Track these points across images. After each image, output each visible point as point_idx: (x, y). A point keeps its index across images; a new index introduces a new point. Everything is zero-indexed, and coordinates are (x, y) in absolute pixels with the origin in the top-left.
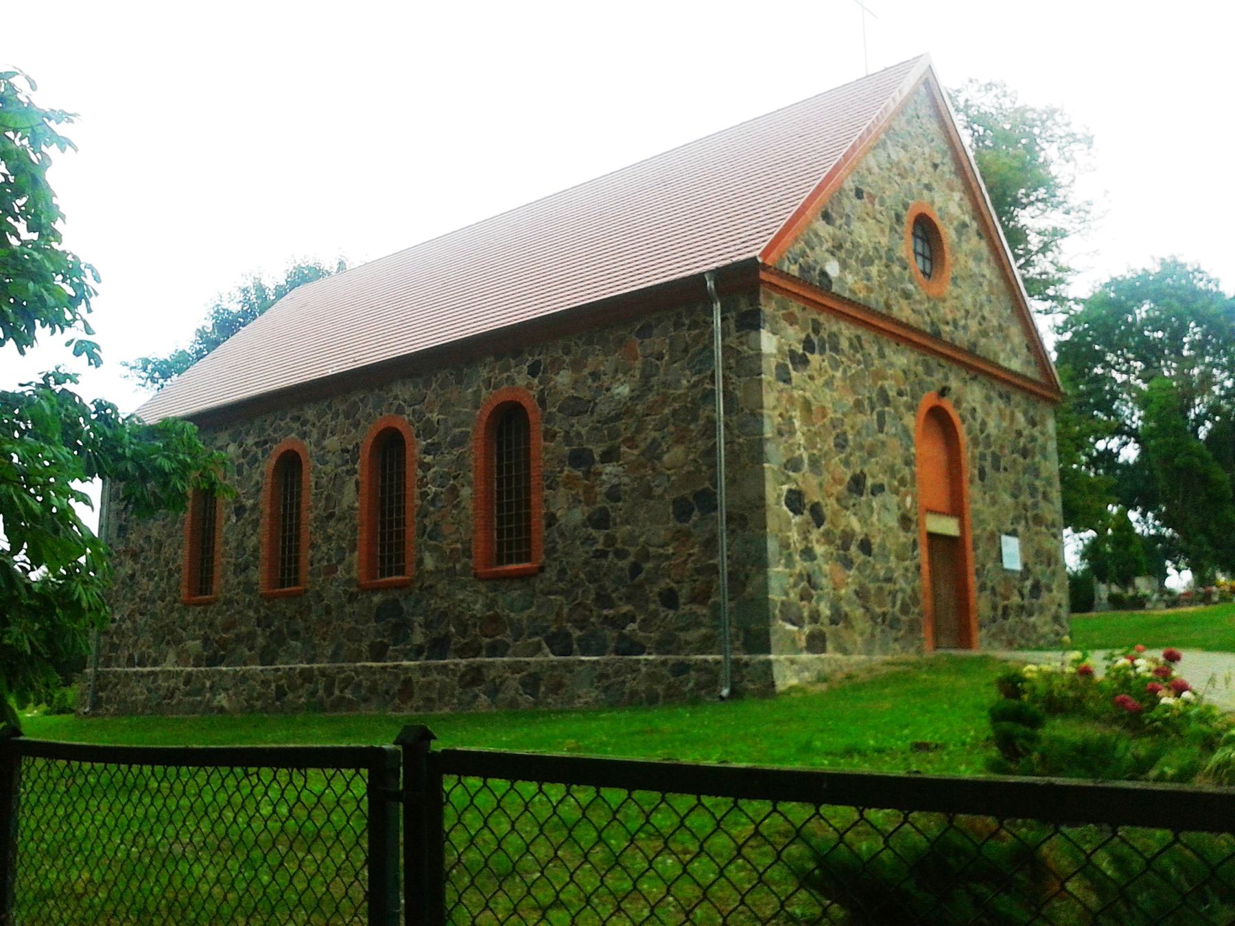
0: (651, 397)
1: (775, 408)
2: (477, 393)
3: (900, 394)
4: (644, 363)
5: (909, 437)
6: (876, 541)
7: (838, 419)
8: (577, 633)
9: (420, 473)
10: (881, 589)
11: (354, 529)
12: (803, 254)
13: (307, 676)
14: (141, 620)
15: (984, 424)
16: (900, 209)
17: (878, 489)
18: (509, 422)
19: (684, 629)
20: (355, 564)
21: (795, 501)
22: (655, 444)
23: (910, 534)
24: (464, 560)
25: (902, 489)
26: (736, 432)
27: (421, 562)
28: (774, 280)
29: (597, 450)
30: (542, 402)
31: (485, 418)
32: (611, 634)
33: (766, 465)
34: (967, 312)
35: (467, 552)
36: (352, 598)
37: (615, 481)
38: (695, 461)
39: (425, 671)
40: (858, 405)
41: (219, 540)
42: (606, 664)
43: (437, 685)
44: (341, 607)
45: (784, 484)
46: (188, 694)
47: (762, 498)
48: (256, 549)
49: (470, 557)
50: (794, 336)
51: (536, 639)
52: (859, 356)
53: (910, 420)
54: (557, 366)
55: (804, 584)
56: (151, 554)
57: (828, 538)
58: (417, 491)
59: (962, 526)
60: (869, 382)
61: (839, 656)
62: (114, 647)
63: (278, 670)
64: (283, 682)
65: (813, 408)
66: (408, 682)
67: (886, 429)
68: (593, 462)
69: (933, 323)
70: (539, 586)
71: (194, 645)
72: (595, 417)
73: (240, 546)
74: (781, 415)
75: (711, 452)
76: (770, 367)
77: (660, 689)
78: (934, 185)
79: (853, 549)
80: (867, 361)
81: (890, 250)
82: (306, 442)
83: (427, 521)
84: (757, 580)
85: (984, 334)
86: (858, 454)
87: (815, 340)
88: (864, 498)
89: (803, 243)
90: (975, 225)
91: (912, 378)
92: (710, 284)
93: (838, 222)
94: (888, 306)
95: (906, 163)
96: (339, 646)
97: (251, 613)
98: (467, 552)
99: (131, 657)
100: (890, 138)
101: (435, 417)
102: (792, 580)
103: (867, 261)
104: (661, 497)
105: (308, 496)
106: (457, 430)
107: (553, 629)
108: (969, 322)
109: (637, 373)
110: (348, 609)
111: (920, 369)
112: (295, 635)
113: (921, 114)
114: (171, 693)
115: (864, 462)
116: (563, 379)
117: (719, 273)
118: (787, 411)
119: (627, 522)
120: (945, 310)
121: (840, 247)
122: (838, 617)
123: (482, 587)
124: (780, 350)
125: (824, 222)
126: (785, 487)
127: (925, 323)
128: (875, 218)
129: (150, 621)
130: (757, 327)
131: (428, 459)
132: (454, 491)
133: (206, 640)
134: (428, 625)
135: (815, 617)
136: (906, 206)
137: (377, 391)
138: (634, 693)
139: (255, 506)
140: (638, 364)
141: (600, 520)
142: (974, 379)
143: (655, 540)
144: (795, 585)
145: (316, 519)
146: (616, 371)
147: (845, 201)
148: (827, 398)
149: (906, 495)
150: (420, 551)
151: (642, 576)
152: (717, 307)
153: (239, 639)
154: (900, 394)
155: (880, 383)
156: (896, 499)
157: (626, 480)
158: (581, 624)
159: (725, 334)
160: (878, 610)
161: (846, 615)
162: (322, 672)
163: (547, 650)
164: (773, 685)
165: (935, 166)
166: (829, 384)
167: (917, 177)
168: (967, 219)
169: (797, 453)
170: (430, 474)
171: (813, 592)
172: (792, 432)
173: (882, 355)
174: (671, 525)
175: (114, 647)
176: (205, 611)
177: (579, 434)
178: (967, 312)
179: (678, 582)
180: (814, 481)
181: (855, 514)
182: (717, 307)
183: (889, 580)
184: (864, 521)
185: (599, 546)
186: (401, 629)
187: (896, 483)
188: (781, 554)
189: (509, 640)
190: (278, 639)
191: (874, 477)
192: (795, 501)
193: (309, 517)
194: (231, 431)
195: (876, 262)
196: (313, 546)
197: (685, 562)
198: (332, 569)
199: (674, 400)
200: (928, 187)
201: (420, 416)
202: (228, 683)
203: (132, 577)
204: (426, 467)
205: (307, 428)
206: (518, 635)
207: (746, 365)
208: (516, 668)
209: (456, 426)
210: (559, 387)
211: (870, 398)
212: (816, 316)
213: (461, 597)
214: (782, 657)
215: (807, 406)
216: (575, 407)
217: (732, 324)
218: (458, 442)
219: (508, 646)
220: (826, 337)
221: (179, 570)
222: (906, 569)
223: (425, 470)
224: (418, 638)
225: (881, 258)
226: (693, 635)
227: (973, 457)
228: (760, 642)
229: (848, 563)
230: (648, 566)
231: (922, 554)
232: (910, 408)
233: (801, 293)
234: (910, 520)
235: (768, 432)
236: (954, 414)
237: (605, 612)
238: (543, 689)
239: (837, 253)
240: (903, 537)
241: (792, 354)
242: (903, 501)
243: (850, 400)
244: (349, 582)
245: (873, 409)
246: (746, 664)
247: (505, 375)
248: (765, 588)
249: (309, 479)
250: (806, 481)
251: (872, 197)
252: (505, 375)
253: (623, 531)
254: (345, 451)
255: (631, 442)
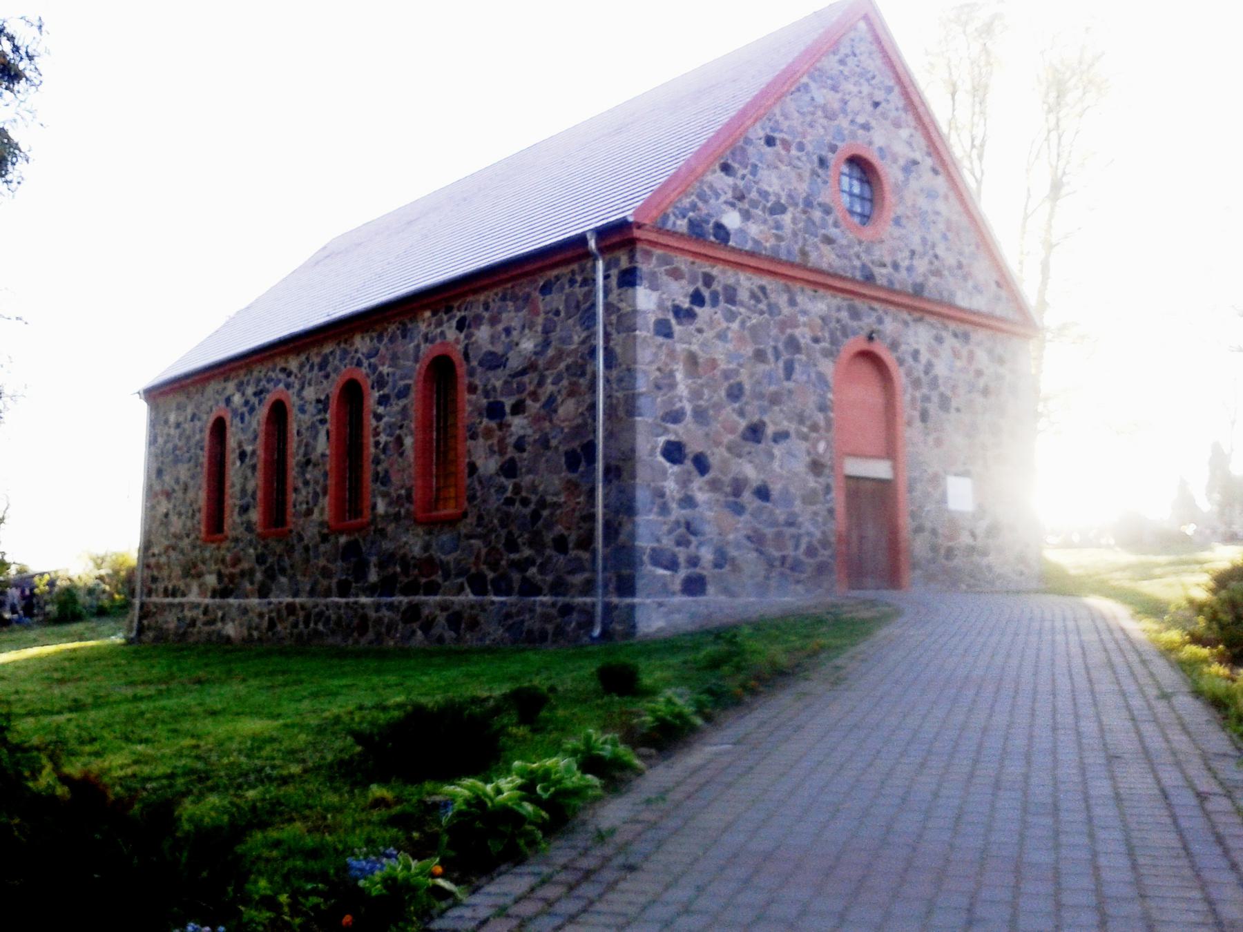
0: (551, 352)
1: (652, 362)
2: (418, 346)
3: (816, 340)
4: (546, 319)
5: (826, 383)
6: (776, 489)
7: (732, 371)
8: (491, 575)
9: (374, 423)
10: (779, 535)
11: (326, 474)
12: (694, 207)
13: (291, 608)
14: (173, 554)
15: (929, 367)
16: (825, 153)
17: (781, 436)
18: (442, 372)
19: (572, 572)
20: (325, 509)
21: (674, 452)
22: (551, 399)
23: (821, 480)
24: (407, 505)
25: (814, 435)
26: (615, 386)
27: (374, 507)
28: (653, 236)
29: (508, 403)
30: (466, 355)
31: (423, 372)
32: (516, 576)
33: (638, 419)
34: (913, 253)
35: (409, 497)
36: (325, 538)
37: (521, 432)
38: (582, 414)
39: (378, 607)
40: (760, 356)
41: (228, 484)
42: (512, 605)
43: (386, 620)
44: (316, 546)
45: (658, 435)
46: (205, 624)
47: (633, 450)
48: (254, 493)
49: (411, 502)
50: (679, 293)
51: (460, 580)
52: (762, 306)
53: (827, 367)
54: (478, 320)
55: (682, 530)
56: (179, 494)
57: (714, 485)
58: (372, 440)
59: (895, 468)
60: (774, 332)
61: (722, 598)
62: (154, 579)
63: (270, 603)
64: (274, 614)
65: (701, 360)
66: (364, 618)
67: (794, 376)
68: (503, 414)
69: (864, 266)
70: (464, 531)
71: (211, 580)
72: (507, 372)
73: (243, 491)
74: (659, 369)
75: (593, 407)
76: (647, 324)
77: (550, 627)
78: (873, 123)
79: (747, 496)
80: (773, 309)
81: (809, 195)
82: (290, 392)
83: (380, 468)
84: (627, 528)
85: (937, 273)
86: (756, 403)
87: (706, 293)
88: (762, 446)
89: (693, 197)
90: (929, 162)
91: (833, 325)
92: (592, 244)
93: (741, 172)
94: (804, 253)
95: (836, 106)
96: (316, 583)
97: (251, 551)
98: (409, 497)
99: (166, 589)
100: (815, 81)
101: (385, 369)
102: (665, 528)
103: (778, 209)
104: (557, 448)
105: (293, 444)
106: (402, 383)
107: (473, 570)
108: (915, 262)
109: (539, 329)
110: (322, 548)
111: (844, 315)
112: (283, 571)
113: (857, 52)
114: (193, 623)
115: (763, 410)
116: (483, 333)
117: (603, 233)
118: (667, 365)
119: (529, 472)
120: (880, 252)
121: (741, 198)
122: (722, 559)
123: (420, 530)
124: (661, 306)
125: (722, 174)
126: (662, 440)
127: (854, 267)
128: (790, 164)
129: (181, 557)
130: (633, 284)
131: (381, 410)
132: (399, 441)
133: (220, 576)
134: (381, 566)
135: (694, 561)
136: (833, 149)
137: (342, 345)
138: (530, 632)
139: (254, 452)
140: (540, 320)
141: (509, 469)
142: (921, 319)
143: (551, 489)
144: (670, 532)
145: (297, 464)
146: (523, 327)
147: (751, 150)
148: (720, 352)
149: (818, 440)
150: (374, 496)
151: (540, 523)
152: (600, 265)
153: (242, 574)
154: (816, 340)
155: (789, 331)
156: (804, 445)
157: (530, 431)
158: (494, 566)
159: (607, 292)
160: (777, 554)
161: (733, 559)
162: (303, 607)
163: (468, 590)
164: (634, 626)
165: (876, 104)
166: (722, 336)
167: (850, 118)
168: (918, 156)
169: (678, 405)
170: (382, 424)
171: (692, 538)
172: (673, 386)
173: (792, 302)
174: (563, 474)
175: (154, 579)
176: (218, 548)
177: (494, 388)
178: (913, 253)
179: (569, 529)
180: (700, 432)
181: (751, 462)
182: (600, 265)
183: (791, 524)
184: (760, 468)
185: (509, 494)
186: (360, 571)
187: (805, 430)
188: (653, 503)
189: (440, 580)
190: (270, 575)
191: (775, 423)
192: (674, 452)
193: (293, 461)
194: (236, 381)
195: (791, 209)
196: (296, 490)
197: (574, 510)
198: (309, 512)
199: (568, 355)
200: (866, 127)
201: (373, 368)
202: (234, 613)
203: (167, 515)
204: (379, 417)
205: (292, 379)
206: (446, 576)
207: (624, 322)
208: (444, 607)
209: (402, 378)
210: (480, 341)
211: (775, 348)
212: (708, 269)
213: (405, 539)
214: (648, 601)
215: (692, 360)
216: (494, 362)
217: (614, 281)
218: (403, 393)
219: (439, 586)
220: (719, 289)
221: (199, 510)
222: (816, 513)
223: (380, 419)
224: (373, 577)
225: (796, 205)
226: (578, 579)
227: (913, 399)
228: (626, 586)
229: (738, 509)
230: (545, 513)
231: (838, 499)
232: (827, 354)
233: (687, 247)
234: (823, 466)
235: (642, 385)
236: (888, 357)
237: (512, 556)
238: (463, 626)
239: (740, 205)
240: (812, 482)
241: (677, 311)
242: (815, 446)
243: (749, 350)
244: (322, 524)
245: (777, 358)
246: (616, 607)
247: (439, 330)
248: (632, 536)
249: (293, 427)
250: (687, 432)
251: (786, 145)
252: (439, 330)
253: (527, 480)
254: (318, 401)
255: (534, 396)
